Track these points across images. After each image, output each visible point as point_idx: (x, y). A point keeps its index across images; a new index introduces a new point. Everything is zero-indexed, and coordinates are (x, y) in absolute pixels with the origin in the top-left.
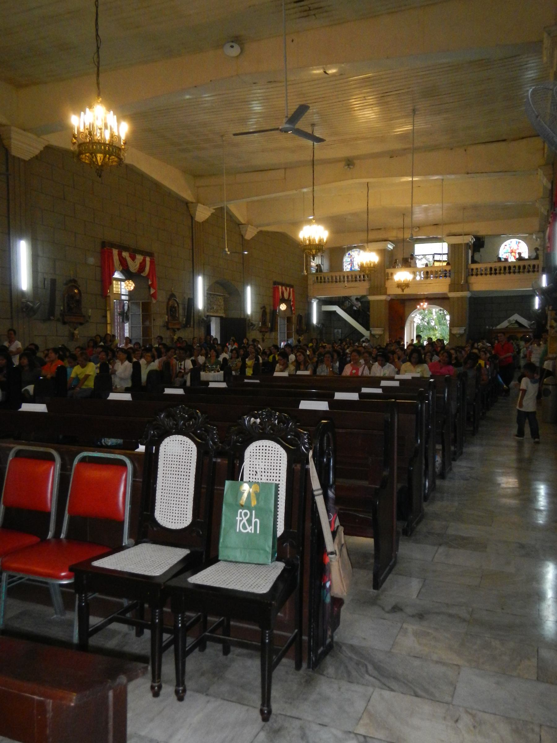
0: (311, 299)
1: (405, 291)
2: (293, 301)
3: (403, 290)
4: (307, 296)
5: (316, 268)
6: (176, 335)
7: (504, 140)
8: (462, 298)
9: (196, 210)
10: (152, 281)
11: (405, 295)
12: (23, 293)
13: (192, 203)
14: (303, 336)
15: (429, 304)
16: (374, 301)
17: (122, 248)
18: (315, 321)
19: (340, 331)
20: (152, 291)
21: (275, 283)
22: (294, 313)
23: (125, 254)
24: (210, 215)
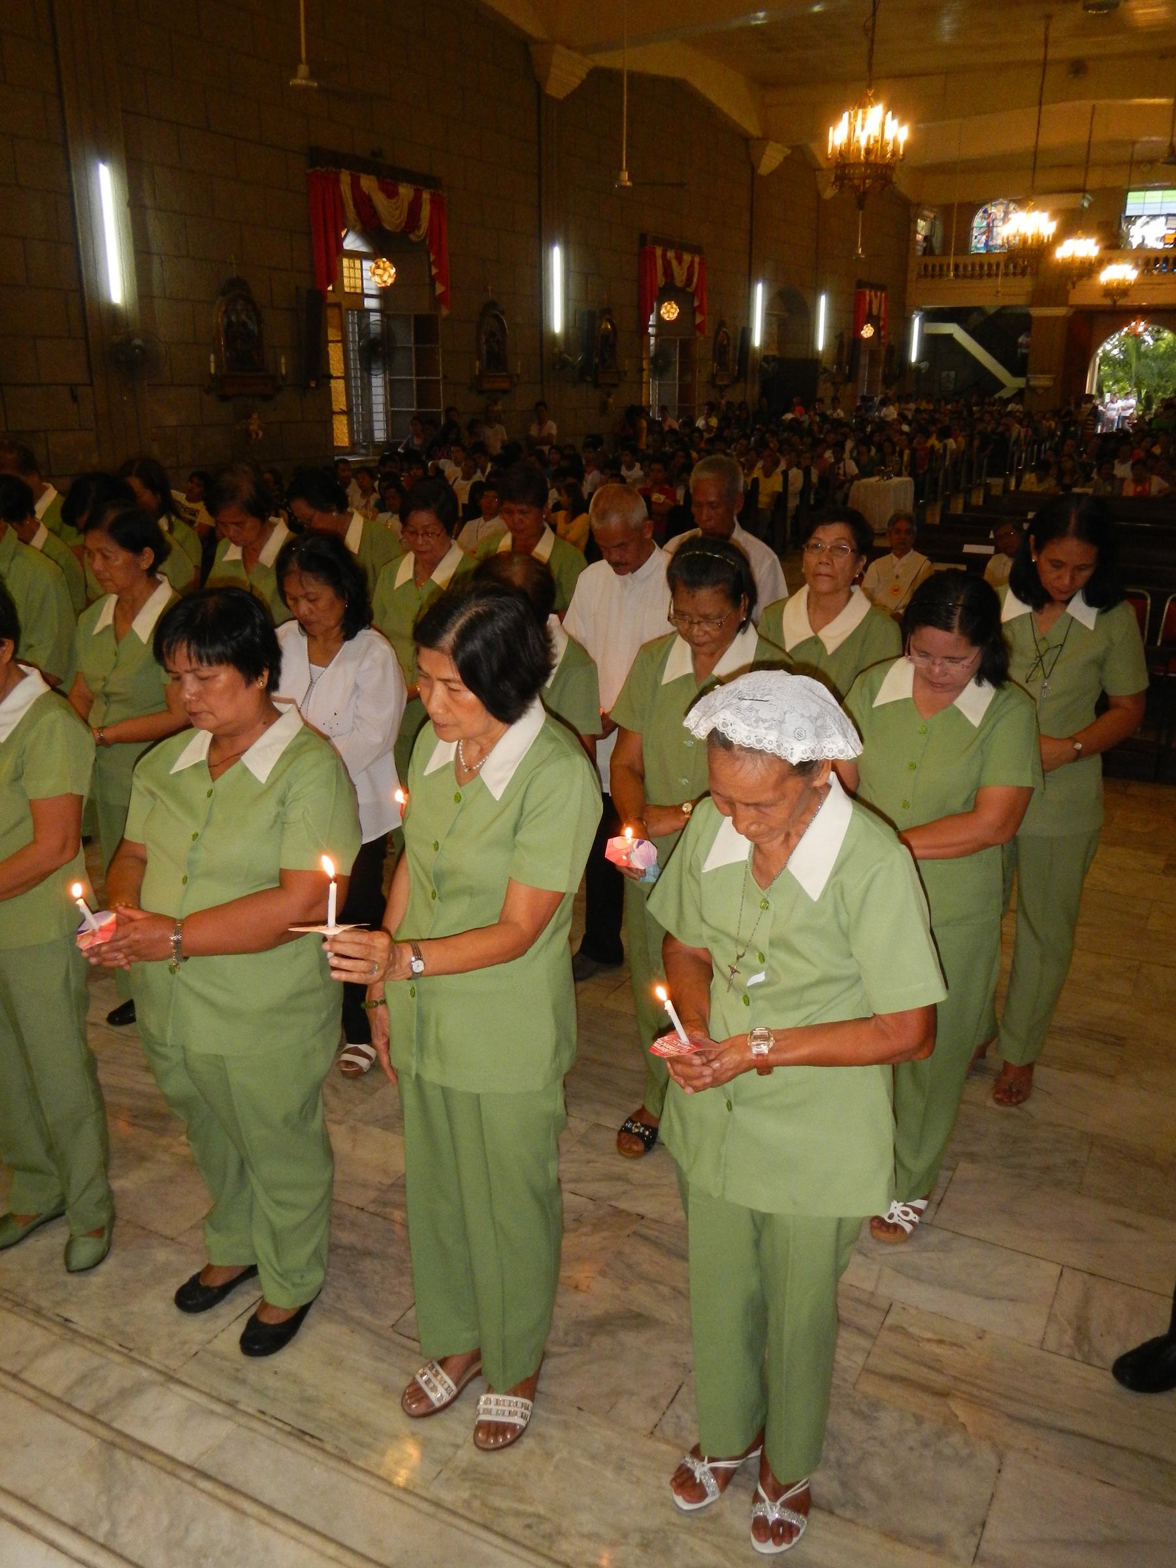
0: (912, 313)
2: (884, 319)
10: (701, 300)
12: (554, 336)
17: (668, 244)
18: (914, 357)
19: (953, 374)
20: (698, 320)
21: (861, 284)
22: (884, 344)
23: (671, 254)
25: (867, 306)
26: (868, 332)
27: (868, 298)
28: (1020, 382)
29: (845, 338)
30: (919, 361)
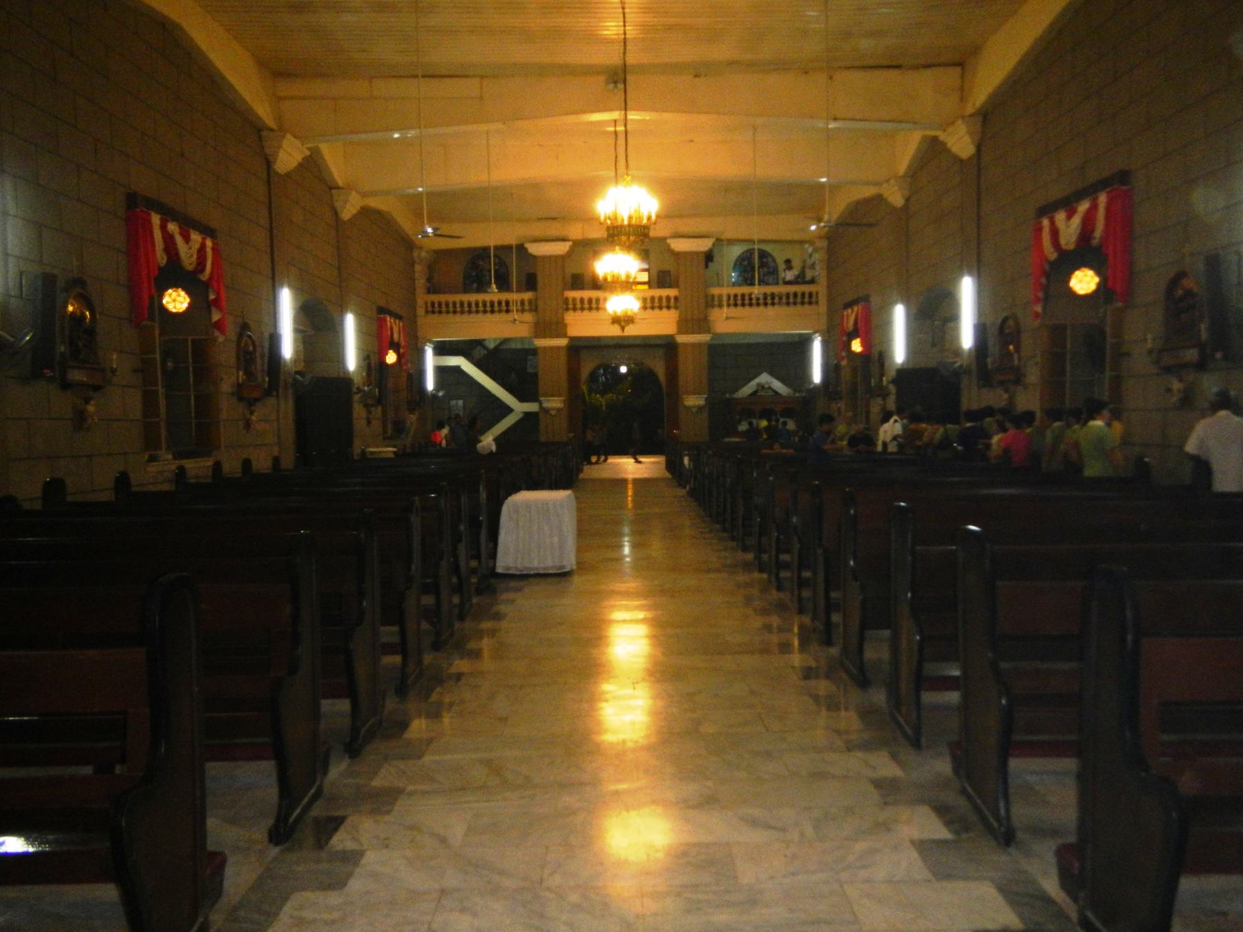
1: (627, 329)
2: (404, 347)
3: (623, 329)
4: (416, 337)
6: (256, 414)
7: (898, 67)
8: (700, 345)
9: (280, 147)
10: (218, 294)
11: (628, 337)
13: (272, 130)
16: (545, 348)
17: (168, 213)
18: (430, 385)
19: (461, 402)
20: (216, 316)
21: (381, 310)
23: (172, 227)
24: (300, 160)
25: (389, 332)
26: (391, 358)
27: (389, 324)
28: (531, 407)
29: (373, 361)
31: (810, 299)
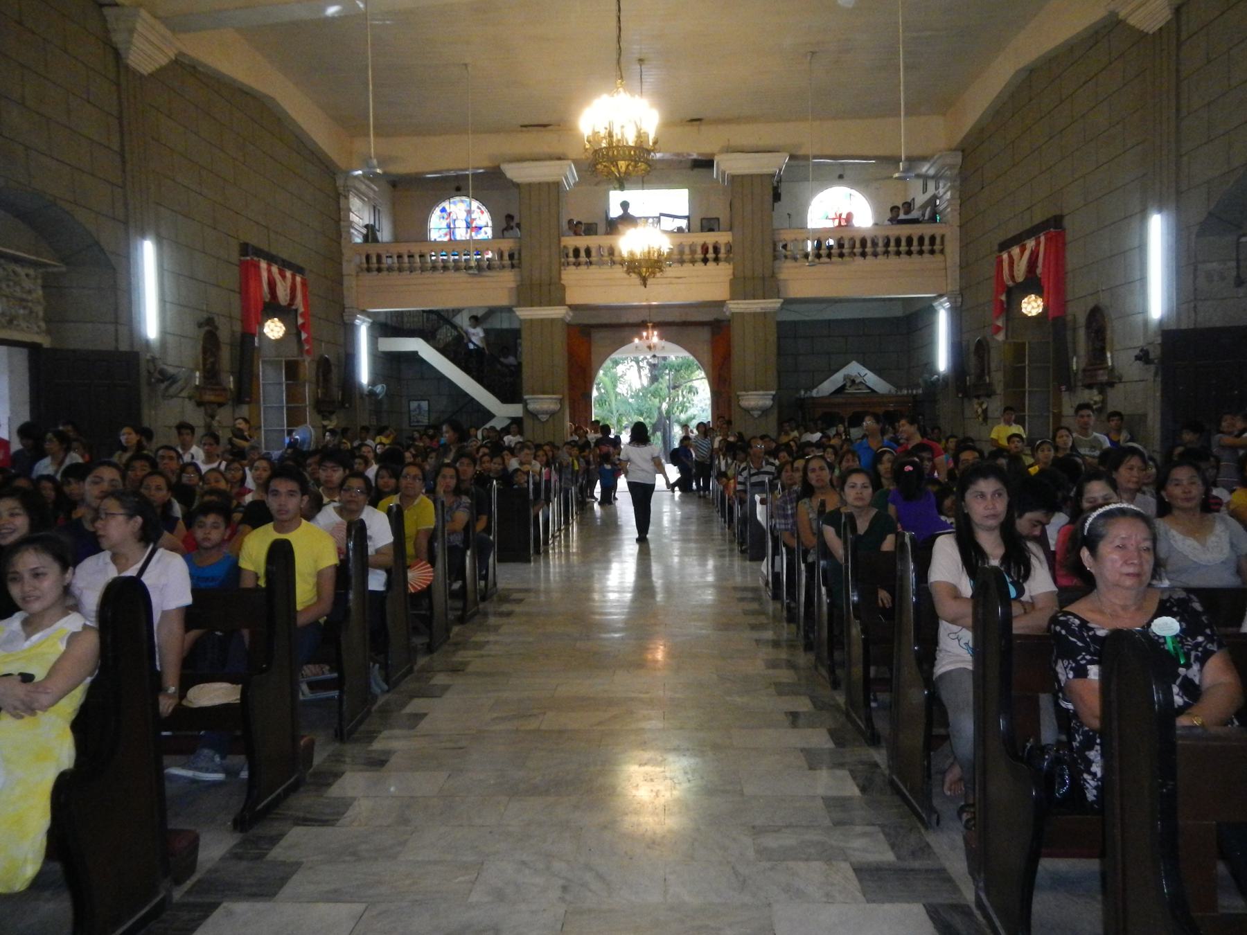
2: (303, 315)
5: (364, 231)
8: (765, 314)
14: (334, 417)
15: (661, 337)
18: (364, 375)
19: (425, 404)
21: (245, 249)
22: (308, 352)
26: (274, 329)
27: (265, 275)
28: (515, 410)
30: (373, 383)
31: (931, 246)
